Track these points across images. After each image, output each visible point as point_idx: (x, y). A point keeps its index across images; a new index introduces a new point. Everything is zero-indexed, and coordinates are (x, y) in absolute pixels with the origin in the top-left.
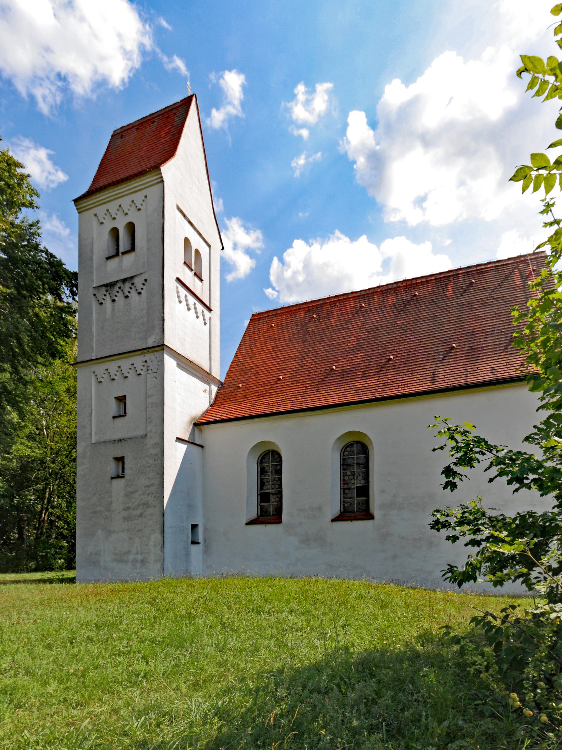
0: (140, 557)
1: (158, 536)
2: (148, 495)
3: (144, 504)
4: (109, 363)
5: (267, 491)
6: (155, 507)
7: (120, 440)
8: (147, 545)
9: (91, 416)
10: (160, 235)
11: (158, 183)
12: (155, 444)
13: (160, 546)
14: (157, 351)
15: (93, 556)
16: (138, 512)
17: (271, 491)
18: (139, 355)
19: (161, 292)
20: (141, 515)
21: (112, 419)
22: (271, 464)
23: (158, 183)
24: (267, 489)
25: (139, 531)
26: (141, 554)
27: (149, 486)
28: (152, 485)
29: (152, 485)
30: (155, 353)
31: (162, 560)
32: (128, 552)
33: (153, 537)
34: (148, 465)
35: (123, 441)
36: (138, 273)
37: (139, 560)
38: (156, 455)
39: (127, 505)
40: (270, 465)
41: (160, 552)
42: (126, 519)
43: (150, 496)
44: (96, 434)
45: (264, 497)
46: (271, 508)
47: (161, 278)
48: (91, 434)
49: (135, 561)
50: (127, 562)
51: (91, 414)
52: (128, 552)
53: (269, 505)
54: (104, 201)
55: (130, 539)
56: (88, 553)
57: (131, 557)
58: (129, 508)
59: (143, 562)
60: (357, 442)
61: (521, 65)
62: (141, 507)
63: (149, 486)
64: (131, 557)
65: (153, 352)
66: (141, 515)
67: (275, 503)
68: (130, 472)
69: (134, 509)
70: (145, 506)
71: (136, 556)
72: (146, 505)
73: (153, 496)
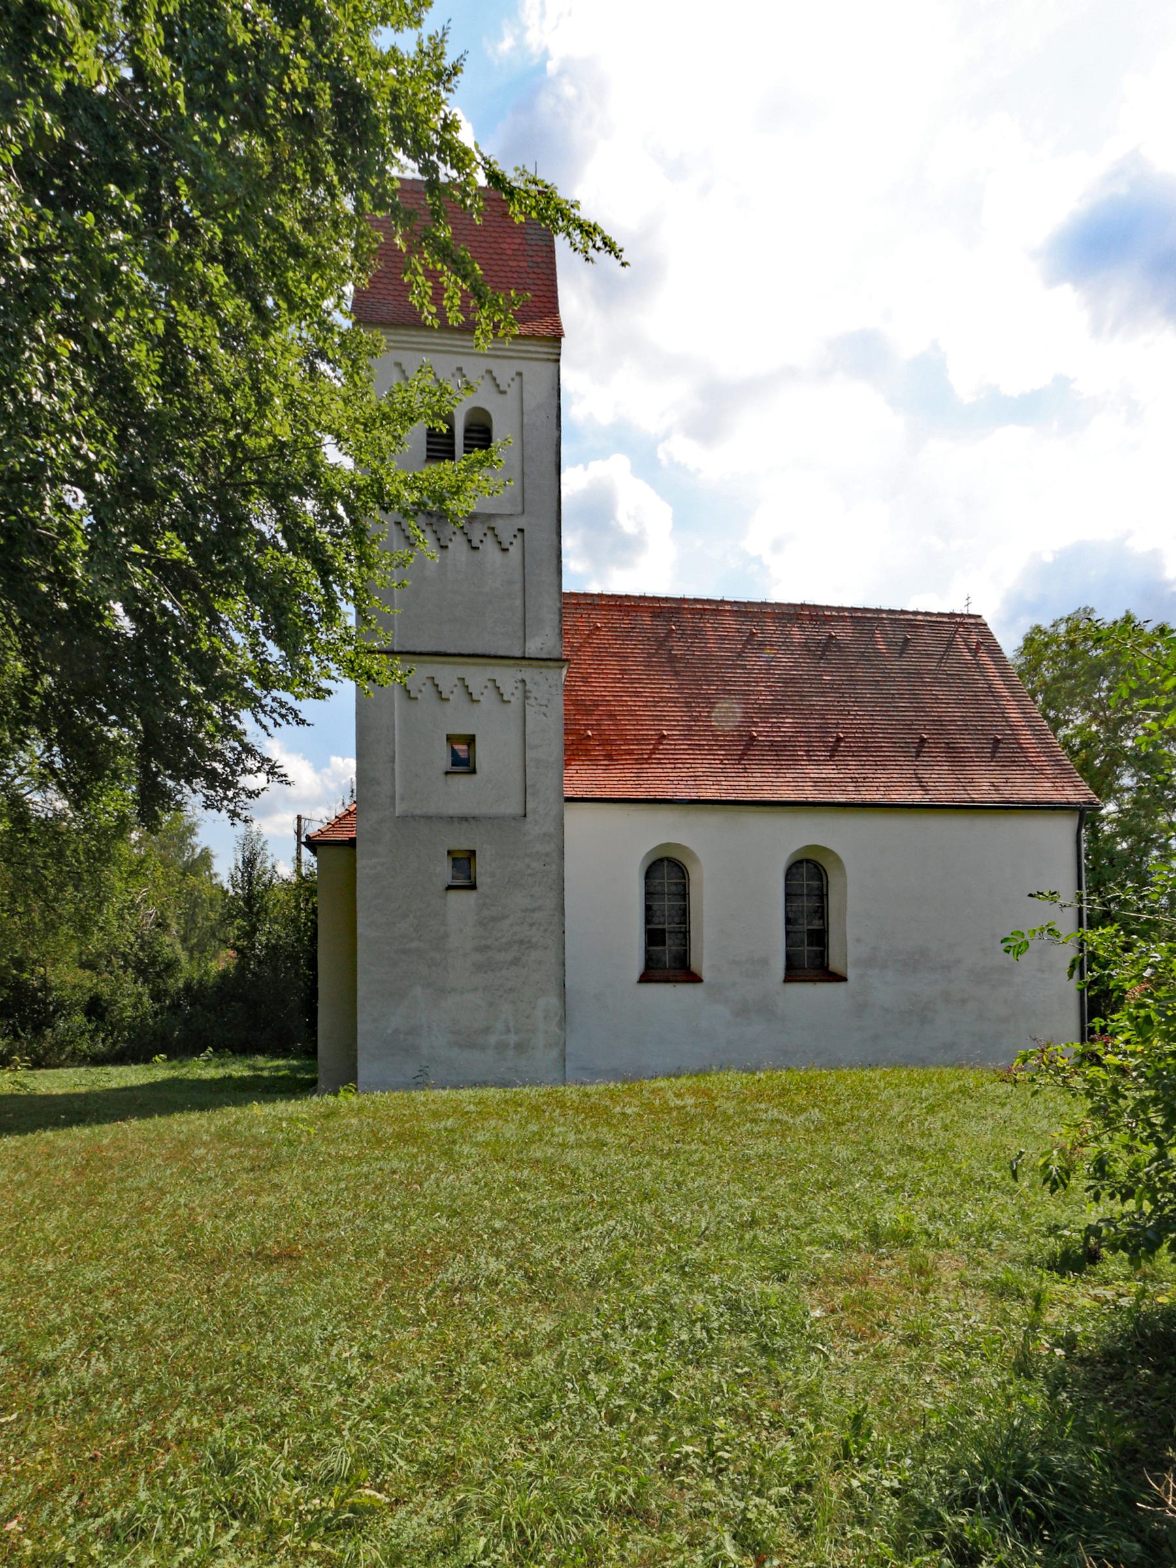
0: (513, 1039)
1: (554, 1001)
2: (532, 925)
3: (522, 942)
4: (441, 666)
5: (660, 927)
6: (546, 948)
7: (465, 819)
8: (528, 1017)
9: (393, 761)
10: (553, 457)
11: (548, 360)
12: (544, 834)
13: (557, 1019)
14: (548, 667)
15: (402, 1037)
16: (509, 956)
17: (666, 926)
18: (508, 666)
19: (555, 562)
20: (515, 962)
21: (443, 776)
22: (666, 881)
23: (548, 360)
24: (659, 923)
25: (511, 990)
26: (516, 1033)
27: (533, 911)
28: (539, 909)
29: (539, 909)
30: (543, 670)
31: (562, 1043)
32: (487, 1030)
33: (542, 1002)
34: (530, 871)
35: (473, 822)
36: (499, 512)
37: (512, 1043)
38: (547, 855)
39: (483, 942)
40: (666, 882)
41: (558, 1031)
42: (479, 968)
43: (534, 928)
44: (402, 799)
45: (653, 937)
46: (667, 953)
47: (554, 536)
48: (393, 797)
49: (501, 1047)
50: (483, 1048)
51: (394, 757)
52: (487, 1030)
53: (664, 951)
54: (422, 347)
55: (491, 1004)
56: (389, 1031)
57: (493, 1039)
58: (488, 948)
59: (520, 1047)
60: (808, 861)
61: (454, 79)
62: (516, 947)
63: (533, 911)
64: (493, 1039)
65: (541, 667)
66: (515, 962)
67: (674, 948)
68: (489, 880)
69: (499, 951)
70: (523, 947)
71: (504, 1037)
72: (527, 944)
73: (542, 928)
